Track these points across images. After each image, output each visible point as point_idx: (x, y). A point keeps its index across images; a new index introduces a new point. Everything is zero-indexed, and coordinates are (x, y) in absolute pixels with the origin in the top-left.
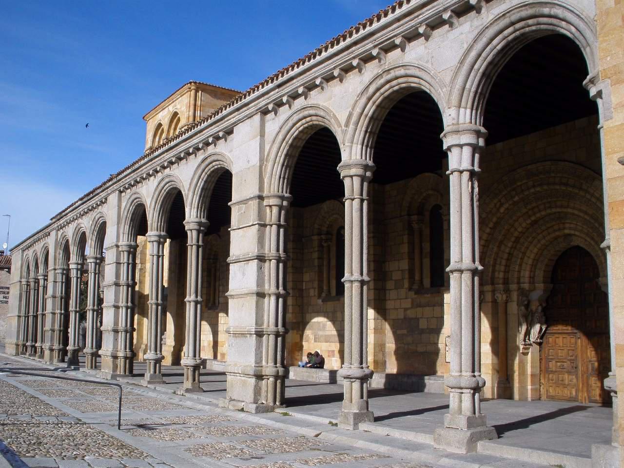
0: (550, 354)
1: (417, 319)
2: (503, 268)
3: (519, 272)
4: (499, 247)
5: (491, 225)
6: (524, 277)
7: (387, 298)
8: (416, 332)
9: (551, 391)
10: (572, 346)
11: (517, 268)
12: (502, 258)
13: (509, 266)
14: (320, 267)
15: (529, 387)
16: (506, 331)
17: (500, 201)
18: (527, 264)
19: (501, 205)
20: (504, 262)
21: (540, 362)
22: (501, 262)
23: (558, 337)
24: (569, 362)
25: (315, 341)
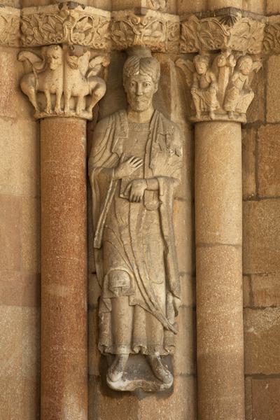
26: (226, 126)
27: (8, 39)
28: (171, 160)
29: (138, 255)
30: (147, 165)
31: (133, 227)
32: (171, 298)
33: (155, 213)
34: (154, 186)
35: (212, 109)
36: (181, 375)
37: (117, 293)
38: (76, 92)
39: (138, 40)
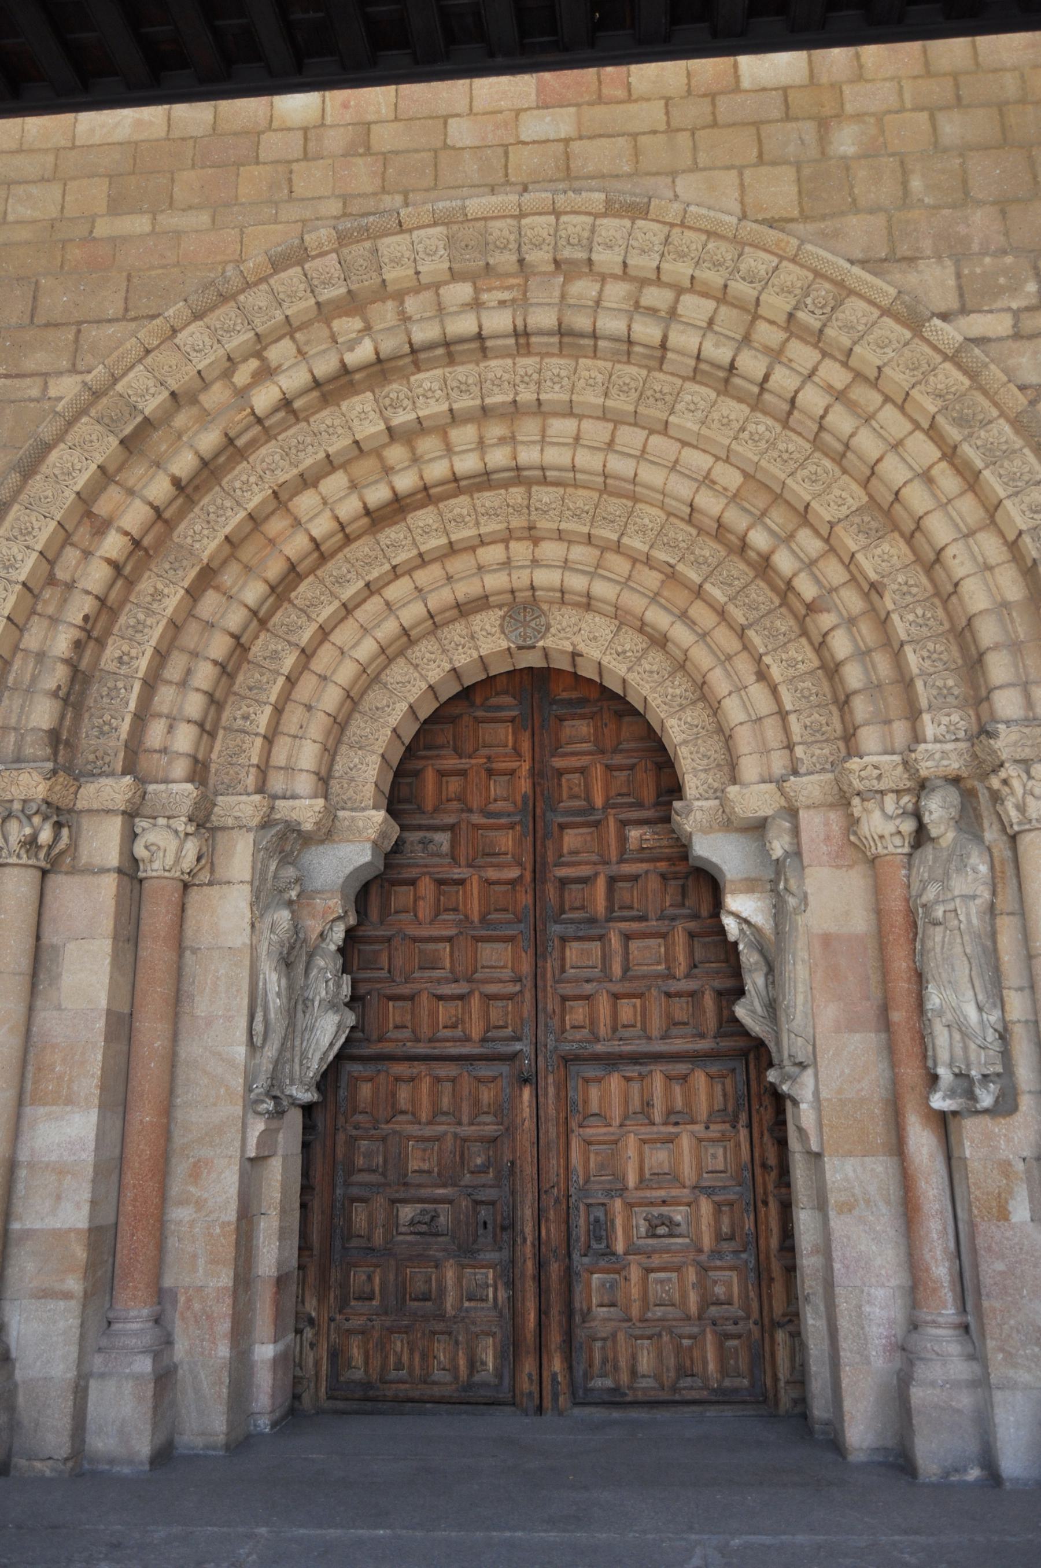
0: (360, 1162)
2: (194, 705)
5: (184, 464)
6: (289, 769)
9: (356, 1353)
11: (263, 718)
16: (175, 1038)
17: (258, 355)
18: (309, 708)
19: (266, 373)
20: (205, 675)
21: (303, 1206)
22: (189, 672)
26: (1032, 834)
27: (830, 799)
28: (970, 878)
29: (944, 975)
30: (946, 888)
31: (938, 949)
32: (985, 1016)
33: (956, 932)
34: (950, 906)
35: (1015, 820)
36: (1030, 1092)
37: (929, 1015)
38: (880, 831)
39: (923, 773)
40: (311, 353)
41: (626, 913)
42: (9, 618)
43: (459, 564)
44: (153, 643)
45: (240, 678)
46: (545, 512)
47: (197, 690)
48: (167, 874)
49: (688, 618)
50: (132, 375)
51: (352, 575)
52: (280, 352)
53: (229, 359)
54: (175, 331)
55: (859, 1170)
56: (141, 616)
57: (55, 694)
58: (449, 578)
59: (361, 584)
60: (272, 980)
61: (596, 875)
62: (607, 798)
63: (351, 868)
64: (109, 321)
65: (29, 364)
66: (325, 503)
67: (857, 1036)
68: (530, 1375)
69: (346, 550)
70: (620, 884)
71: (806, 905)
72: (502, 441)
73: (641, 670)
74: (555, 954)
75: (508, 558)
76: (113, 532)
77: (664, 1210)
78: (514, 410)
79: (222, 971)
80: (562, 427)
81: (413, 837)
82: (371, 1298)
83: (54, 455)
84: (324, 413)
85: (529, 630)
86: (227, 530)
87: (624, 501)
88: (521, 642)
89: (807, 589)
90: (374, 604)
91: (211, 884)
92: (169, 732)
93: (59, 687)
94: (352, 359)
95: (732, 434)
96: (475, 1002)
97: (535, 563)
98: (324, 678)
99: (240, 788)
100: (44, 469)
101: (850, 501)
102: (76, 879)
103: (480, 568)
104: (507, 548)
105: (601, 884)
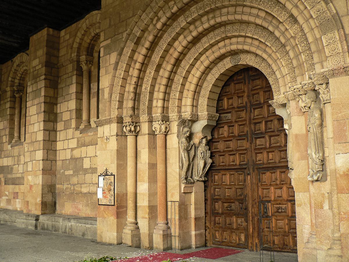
1: (82, 159)
2: (161, 96)
3: (180, 99)
4: (157, 70)
7: (58, 140)
8: (81, 173)
10: (240, 183)
12: (160, 84)
13: (169, 94)
14: (12, 115)
15: (193, 233)
17: (157, 16)
18: (188, 90)
19: (159, 19)
20: (162, 88)
21: (205, 203)
22: (159, 88)
23: (225, 175)
24: (237, 203)
25: (5, 184)
40: (166, 12)
41: (270, 130)
42: (121, 86)
43: (215, 48)
44: (150, 84)
45: (173, 86)
46: (229, 31)
47: (161, 92)
48: (159, 133)
49: (266, 51)
50: (135, 28)
51: (191, 57)
52: (160, 14)
53: (151, 19)
54: (141, 16)
55: (303, 196)
56: (148, 78)
57: (131, 100)
58: (213, 52)
59: (193, 59)
60: (184, 155)
61: (262, 121)
62: (264, 100)
63: (203, 126)
64: (131, 17)
65: (120, 31)
66: (180, 43)
67: (303, 161)
68: (251, 243)
69: (190, 52)
70: (269, 123)
71: (291, 127)
72: (213, 18)
73: (262, 66)
74: (254, 142)
75: (225, 44)
76: (137, 63)
77: (280, 206)
78: (213, 10)
79: (174, 153)
80: (224, 11)
81: (222, 115)
82: (220, 224)
83: (125, 49)
84: (175, 23)
85: (236, 61)
86: (160, 55)
87: (246, 24)
88: (234, 64)
89: (283, 40)
90: (199, 63)
91: (171, 134)
92: (157, 102)
93: (132, 98)
94: (173, 11)
95: (258, 3)
96: (237, 155)
97: (231, 44)
98: (191, 83)
99: (174, 112)
100: (123, 53)
101: (287, 14)
102: (142, 136)
103: (219, 48)
104: (224, 42)
105: (264, 123)
